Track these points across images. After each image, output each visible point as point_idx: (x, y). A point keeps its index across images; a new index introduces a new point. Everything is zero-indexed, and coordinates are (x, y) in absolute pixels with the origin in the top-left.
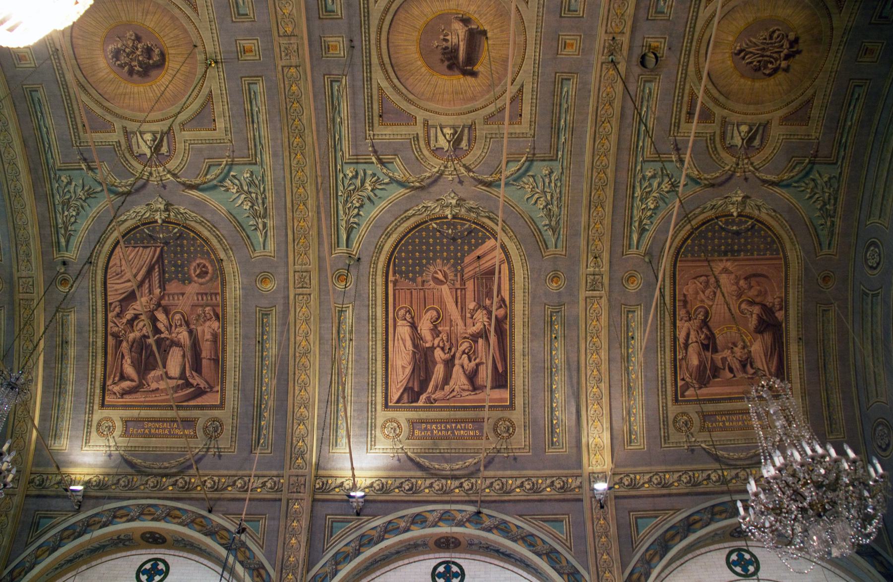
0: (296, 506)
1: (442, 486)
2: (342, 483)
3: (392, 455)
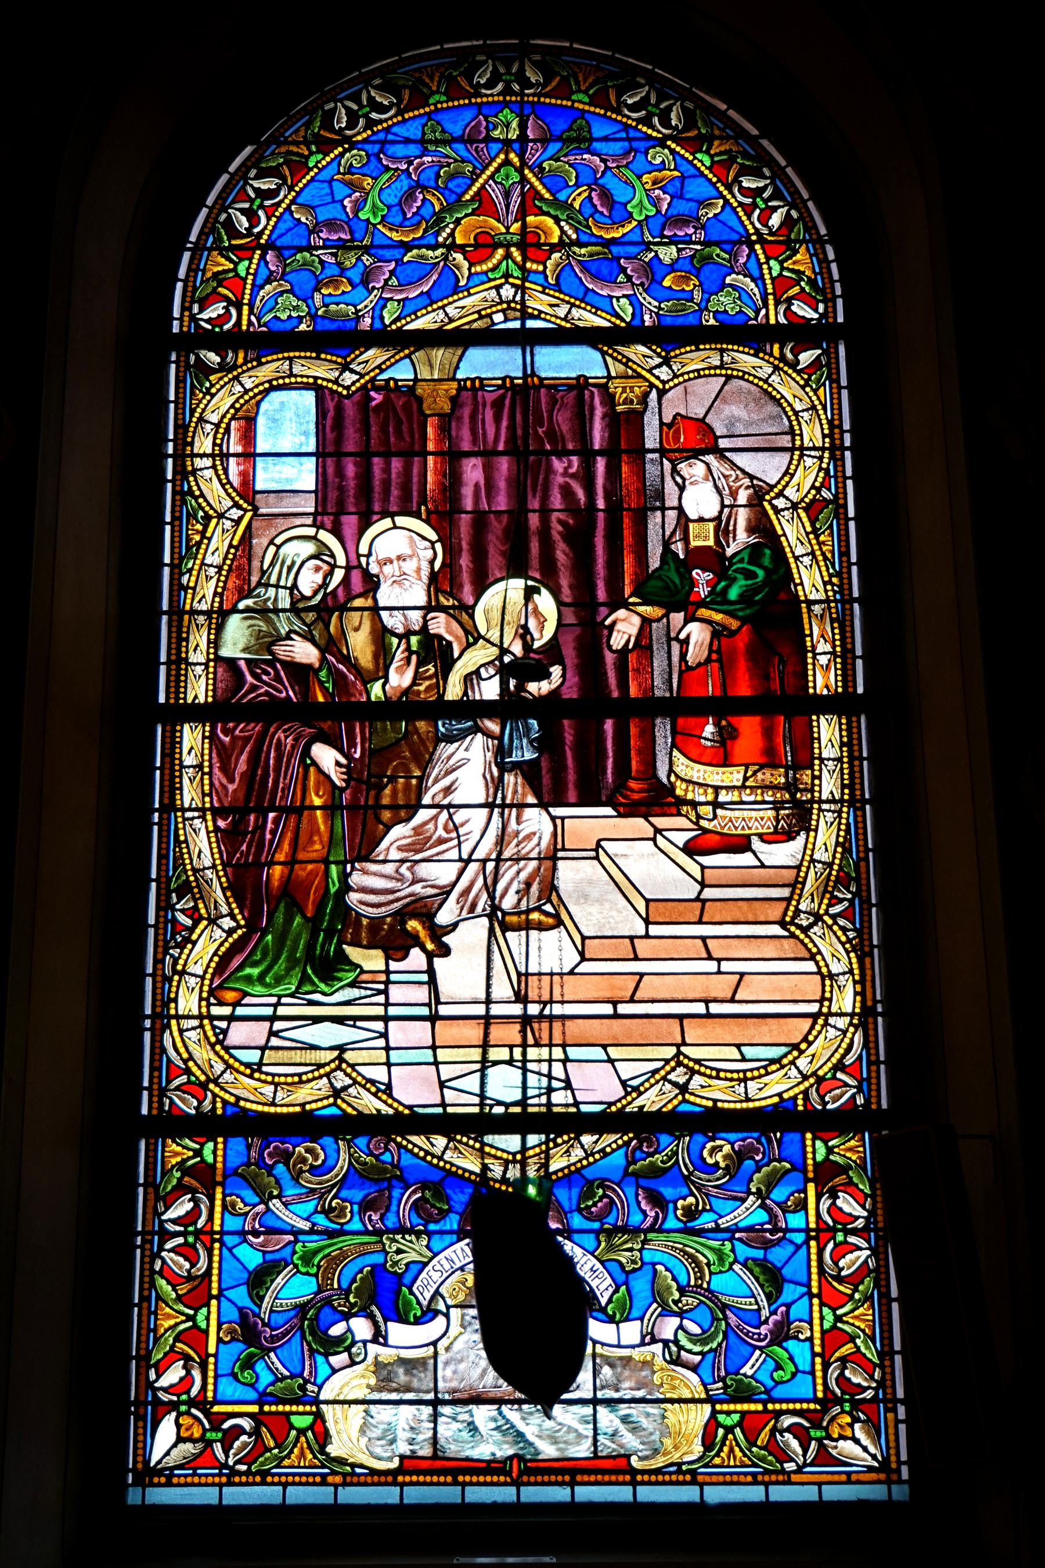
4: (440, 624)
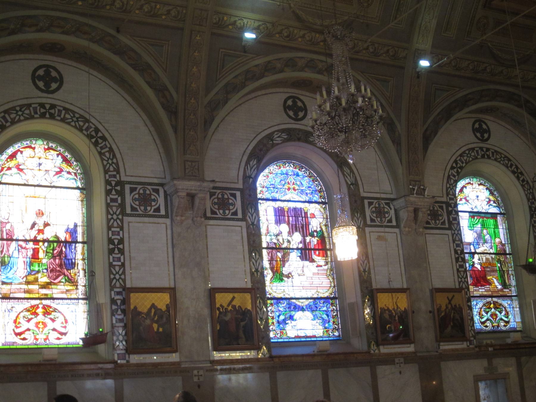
0: (198, 38)
1: (312, 38)
2: (235, 22)
3: (278, 3)
4: (289, 238)
